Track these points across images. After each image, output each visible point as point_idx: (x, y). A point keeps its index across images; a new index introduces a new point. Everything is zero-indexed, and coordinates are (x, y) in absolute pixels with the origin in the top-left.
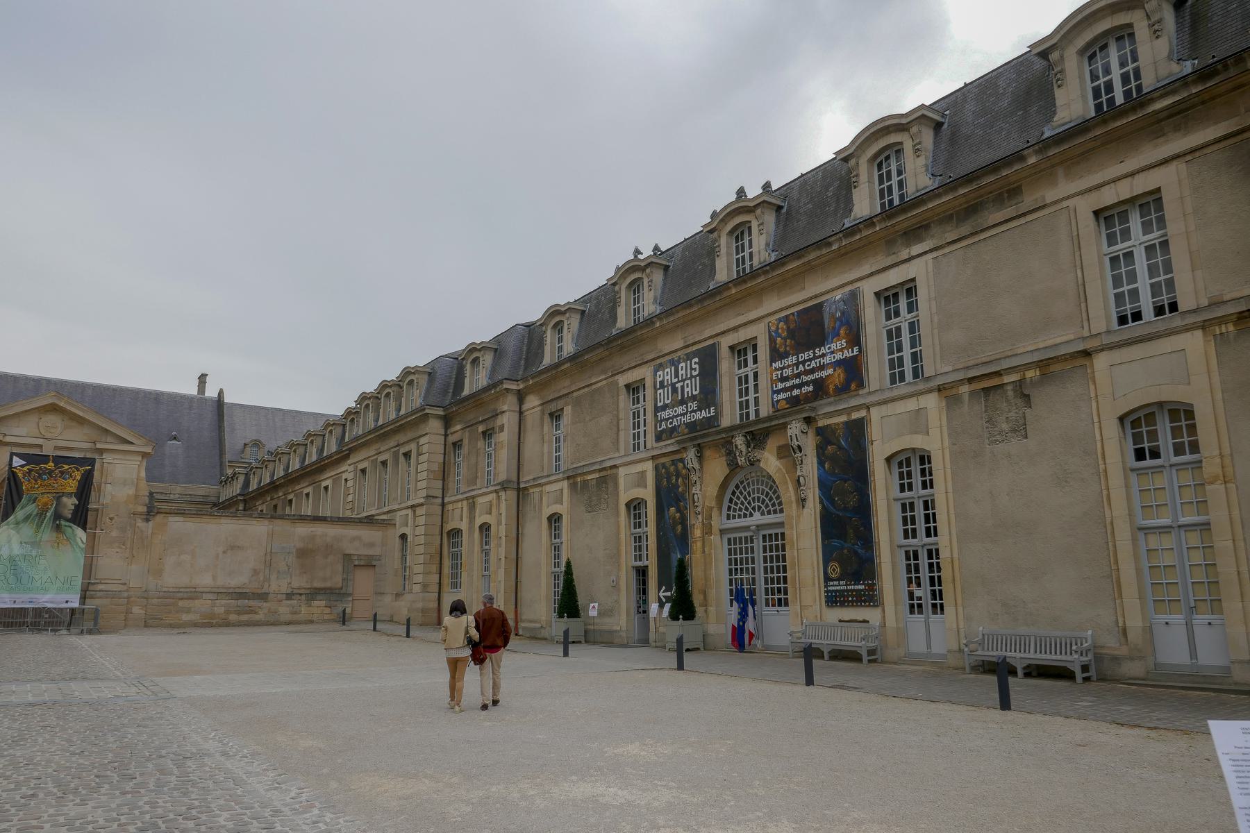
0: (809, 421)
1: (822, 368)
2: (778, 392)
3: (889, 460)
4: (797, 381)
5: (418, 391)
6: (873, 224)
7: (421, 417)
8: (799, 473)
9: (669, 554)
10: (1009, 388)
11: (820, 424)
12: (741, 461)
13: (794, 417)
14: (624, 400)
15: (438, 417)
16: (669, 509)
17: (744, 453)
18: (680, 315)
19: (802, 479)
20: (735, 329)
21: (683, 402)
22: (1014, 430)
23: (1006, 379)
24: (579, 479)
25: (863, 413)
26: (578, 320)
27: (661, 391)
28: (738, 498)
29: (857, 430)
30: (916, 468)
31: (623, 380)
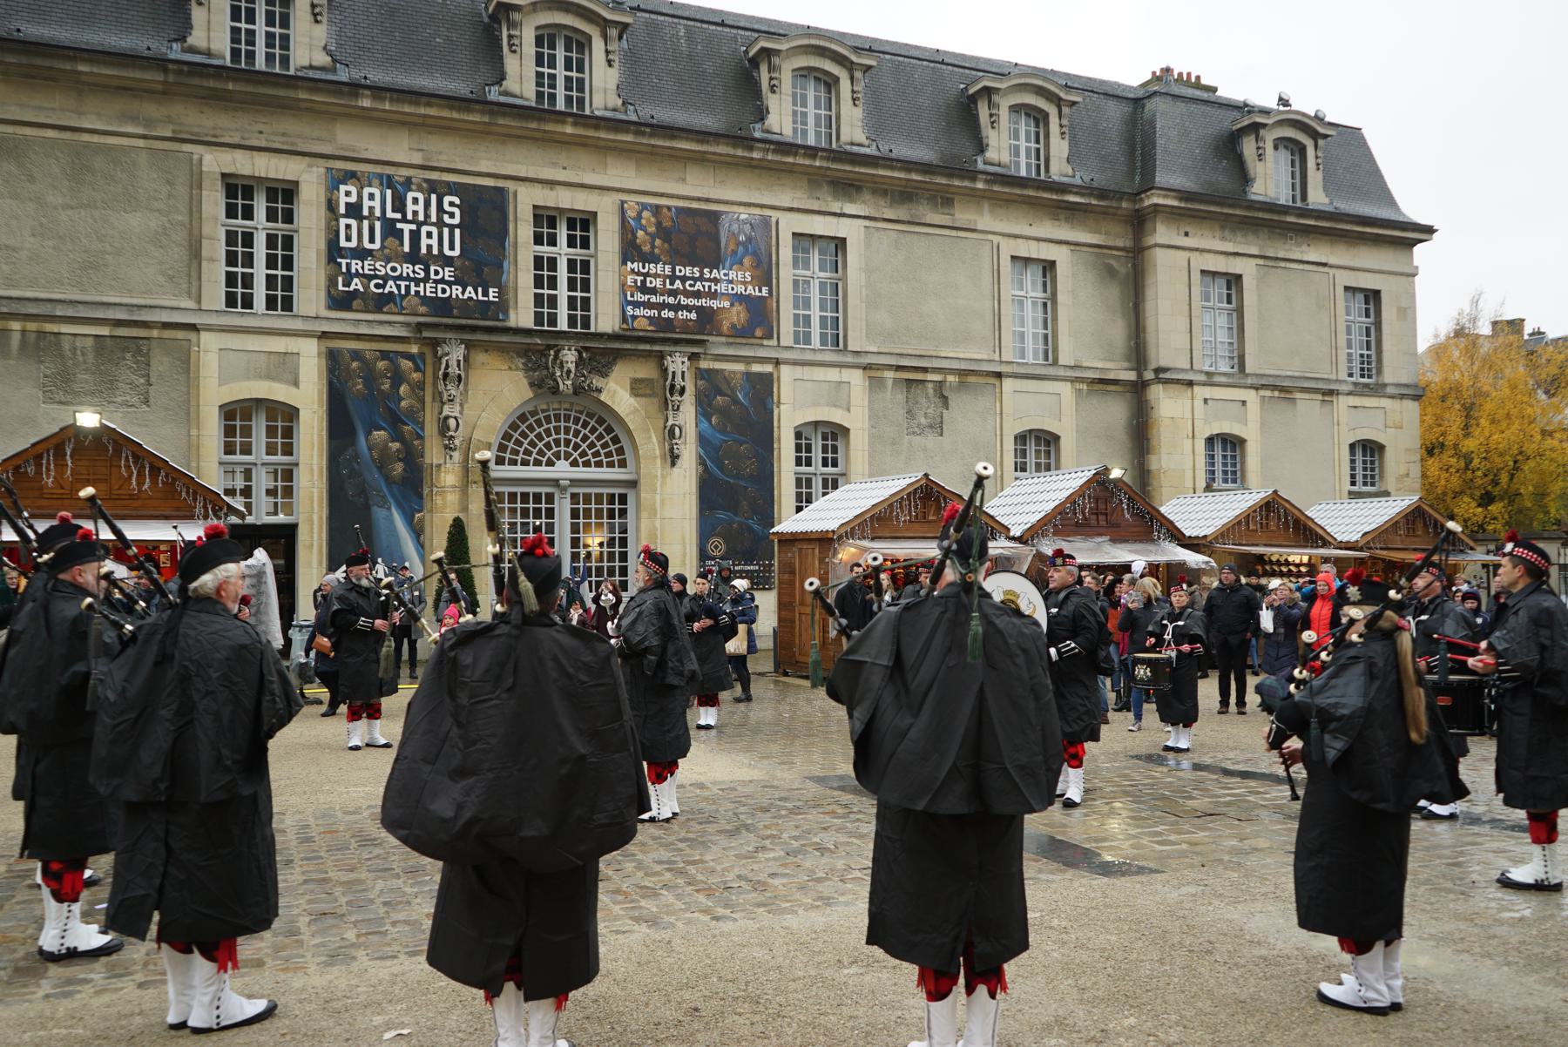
0: (693, 357)
1: (714, 295)
2: (636, 305)
4: (671, 300)
6: (814, 157)
9: (367, 508)
10: (930, 386)
11: (704, 365)
13: (678, 349)
16: (368, 433)
18: (432, 112)
19: (677, 430)
20: (552, 184)
21: (414, 257)
22: (931, 427)
23: (930, 377)
24: (16, 325)
25: (768, 368)
27: (353, 223)
29: (763, 388)
31: (215, 162)
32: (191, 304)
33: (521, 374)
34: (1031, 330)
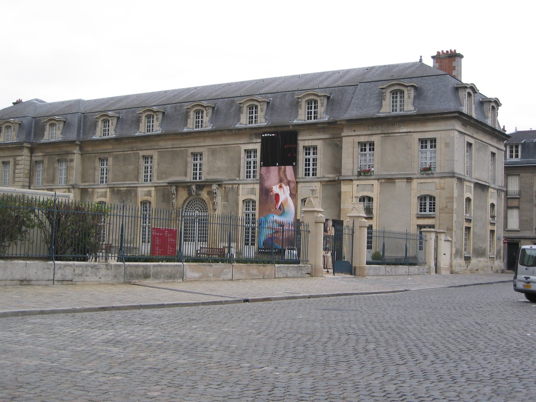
3: (243, 201)
5: (15, 132)
7: (19, 146)
8: (214, 201)
12: (194, 194)
14: (142, 162)
15: (28, 148)
17: (195, 191)
19: (215, 203)
24: (116, 189)
26: (116, 121)
28: (190, 205)
30: (251, 204)
31: (141, 153)
32: (137, 182)
33: (187, 191)
34: (312, 167)
